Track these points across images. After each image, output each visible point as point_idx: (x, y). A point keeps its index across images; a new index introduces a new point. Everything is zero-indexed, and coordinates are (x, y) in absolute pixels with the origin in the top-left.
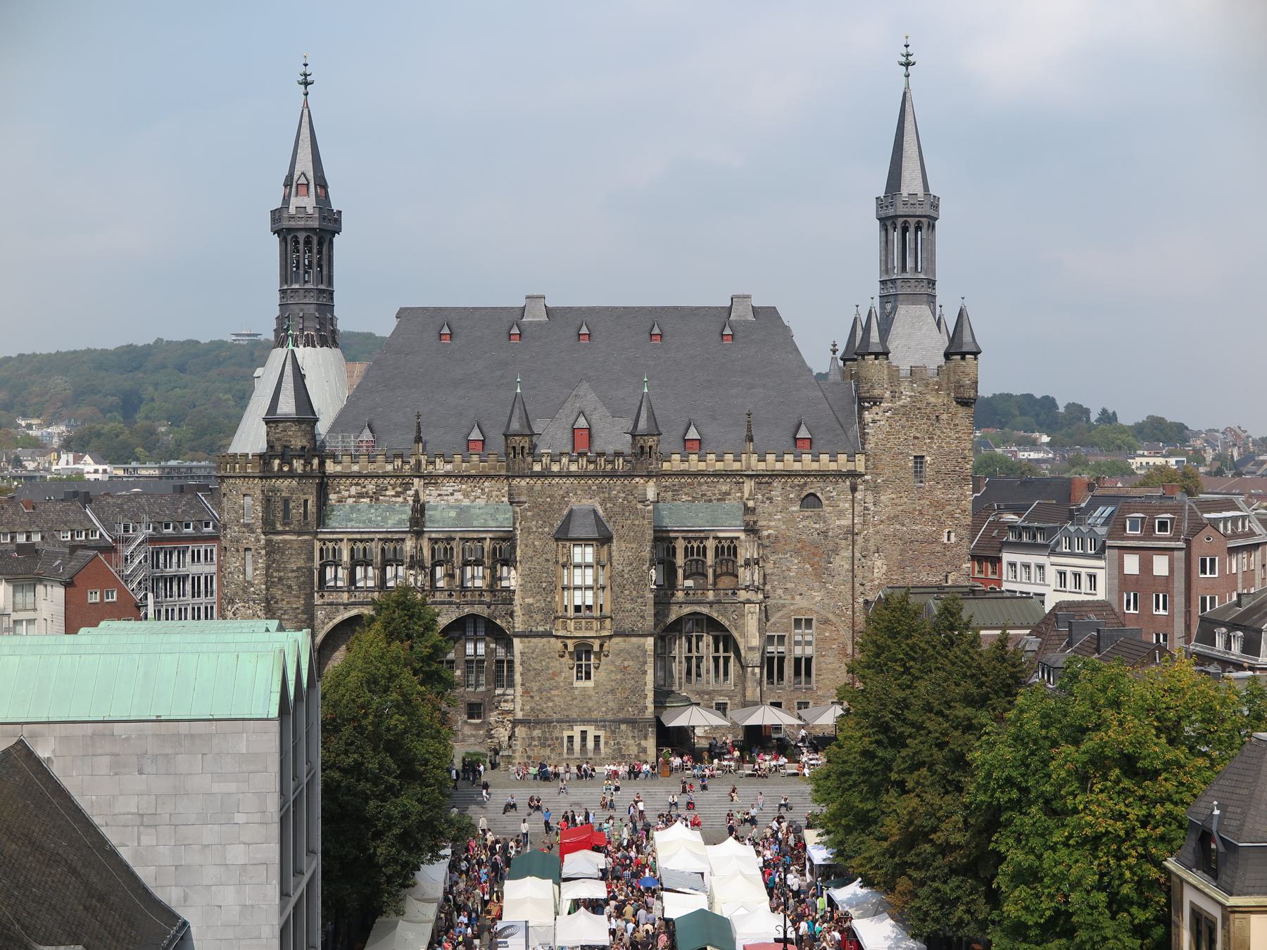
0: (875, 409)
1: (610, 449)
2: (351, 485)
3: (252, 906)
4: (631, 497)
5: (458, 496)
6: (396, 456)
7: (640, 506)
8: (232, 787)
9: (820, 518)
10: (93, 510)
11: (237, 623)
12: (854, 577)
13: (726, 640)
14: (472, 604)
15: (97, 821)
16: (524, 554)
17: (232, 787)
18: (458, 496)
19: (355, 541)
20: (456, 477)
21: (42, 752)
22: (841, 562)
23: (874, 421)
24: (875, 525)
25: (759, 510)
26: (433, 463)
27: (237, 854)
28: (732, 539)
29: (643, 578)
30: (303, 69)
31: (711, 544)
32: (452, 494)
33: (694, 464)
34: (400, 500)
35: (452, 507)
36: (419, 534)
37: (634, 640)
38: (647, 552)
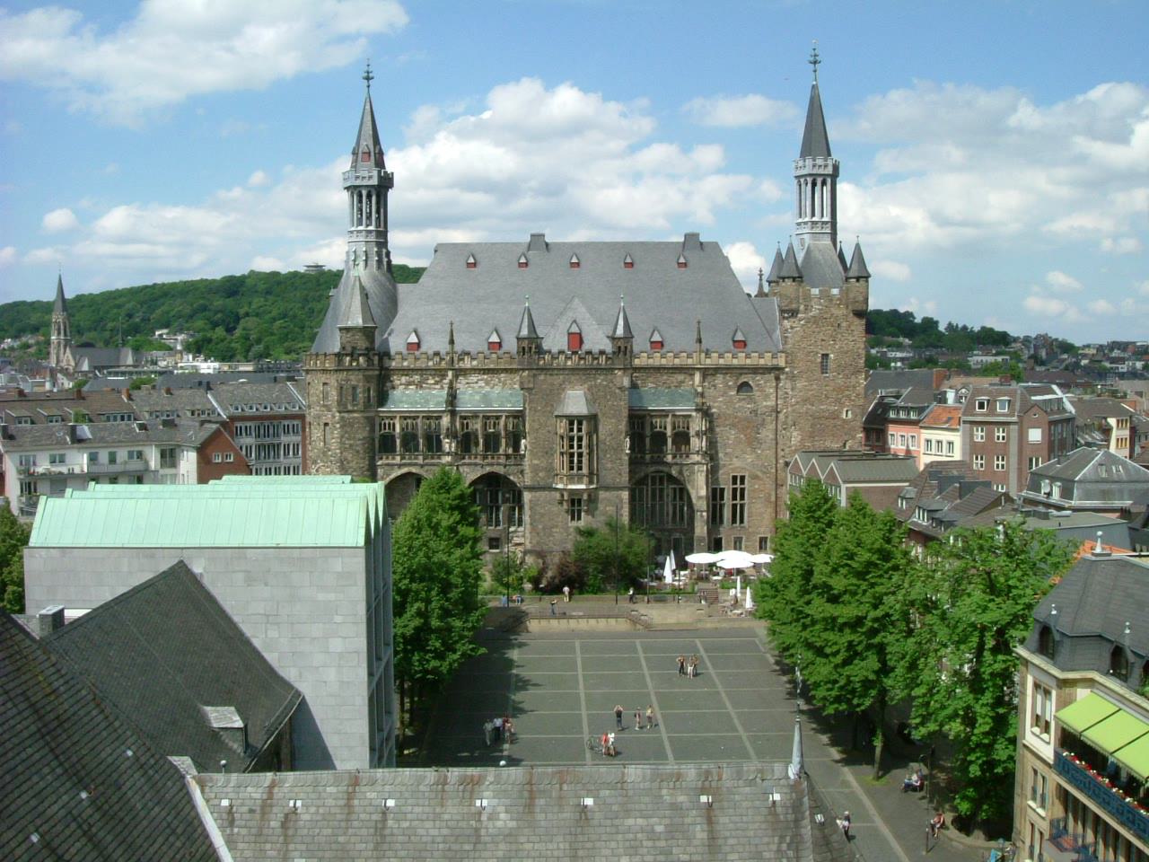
0: (792, 320)
1: (596, 350)
3: (348, 682)
4: (611, 385)
7: (617, 391)
8: (332, 596)
9: (751, 400)
10: (213, 395)
11: (320, 478)
12: (777, 444)
13: (682, 493)
14: (492, 465)
15: (236, 619)
16: (530, 429)
17: (332, 596)
18: (482, 383)
19: (405, 418)
20: (480, 370)
21: (197, 568)
22: (767, 433)
23: (792, 328)
24: (792, 406)
25: (706, 394)
26: (463, 359)
27: (336, 645)
29: (619, 449)
30: (366, 69)
31: (669, 420)
33: (657, 360)
34: (438, 387)
35: (477, 393)
36: (453, 413)
37: (615, 493)
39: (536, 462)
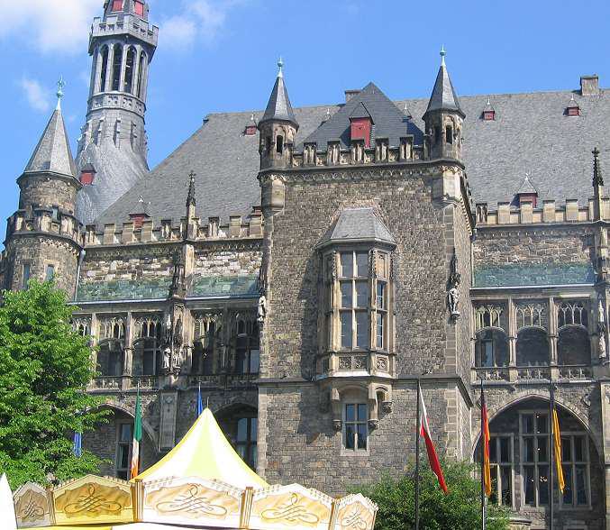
2: (112, 259)
5: (235, 266)
6: (165, 222)
16: (277, 277)
26: (205, 229)
28: (579, 302)
31: (555, 309)
32: (227, 264)
33: (529, 215)
34: (167, 273)
38: (444, 269)
39: (281, 336)
